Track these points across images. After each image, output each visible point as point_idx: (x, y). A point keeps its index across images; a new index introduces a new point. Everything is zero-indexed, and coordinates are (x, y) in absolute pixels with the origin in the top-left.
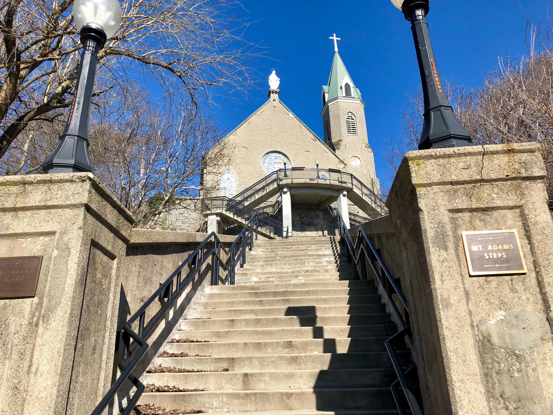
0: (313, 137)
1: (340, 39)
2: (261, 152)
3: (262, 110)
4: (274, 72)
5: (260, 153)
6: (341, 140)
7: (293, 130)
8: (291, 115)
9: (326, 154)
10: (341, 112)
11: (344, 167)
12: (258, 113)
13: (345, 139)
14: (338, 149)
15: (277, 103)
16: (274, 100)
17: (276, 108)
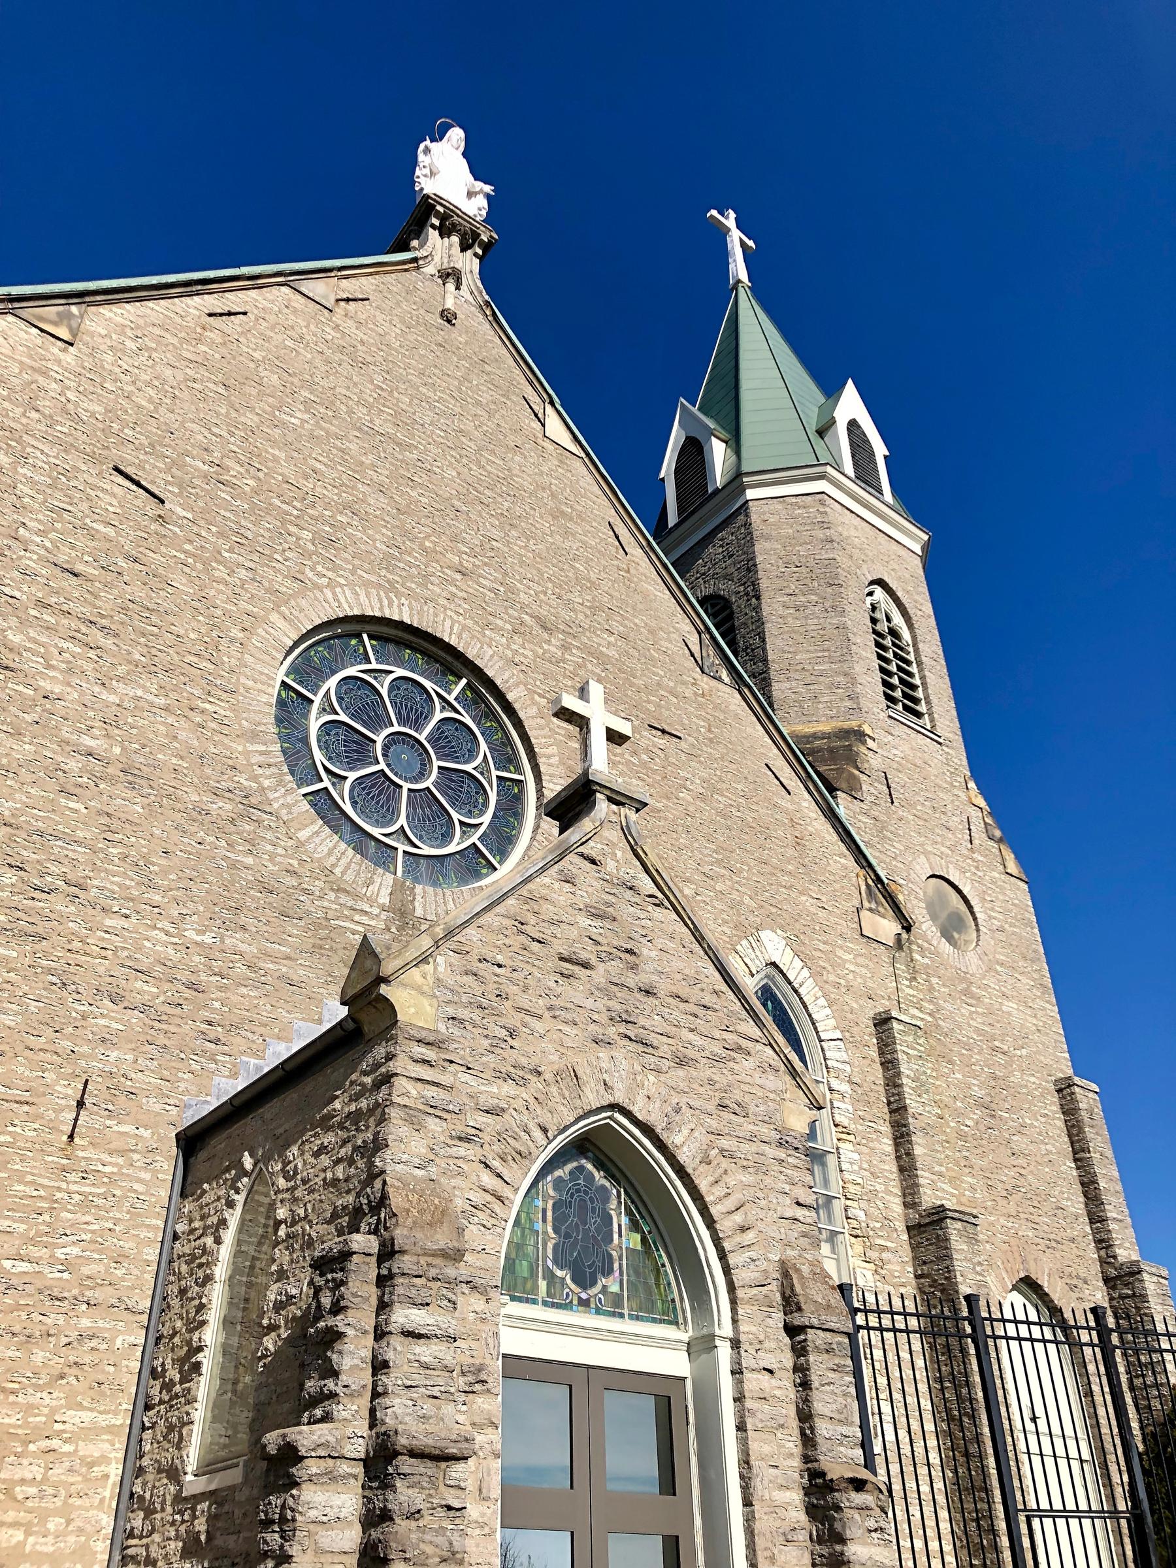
0: (693, 641)
1: (751, 243)
2: (288, 586)
3: (350, 287)
4: (456, 134)
5: (279, 599)
6: (861, 736)
7: (567, 533)
8: (555, 427)
9: (784, 801)
10: (842, 560)
11: (899, 944)
12: (317, 288)
13: (878, 734)
14: (853, 791)
15: (467, 298)
16: (451, 275)
17: (457, 336)
